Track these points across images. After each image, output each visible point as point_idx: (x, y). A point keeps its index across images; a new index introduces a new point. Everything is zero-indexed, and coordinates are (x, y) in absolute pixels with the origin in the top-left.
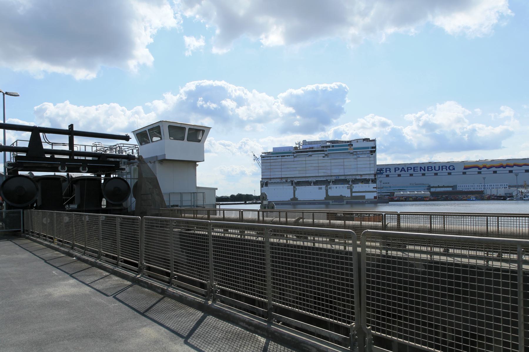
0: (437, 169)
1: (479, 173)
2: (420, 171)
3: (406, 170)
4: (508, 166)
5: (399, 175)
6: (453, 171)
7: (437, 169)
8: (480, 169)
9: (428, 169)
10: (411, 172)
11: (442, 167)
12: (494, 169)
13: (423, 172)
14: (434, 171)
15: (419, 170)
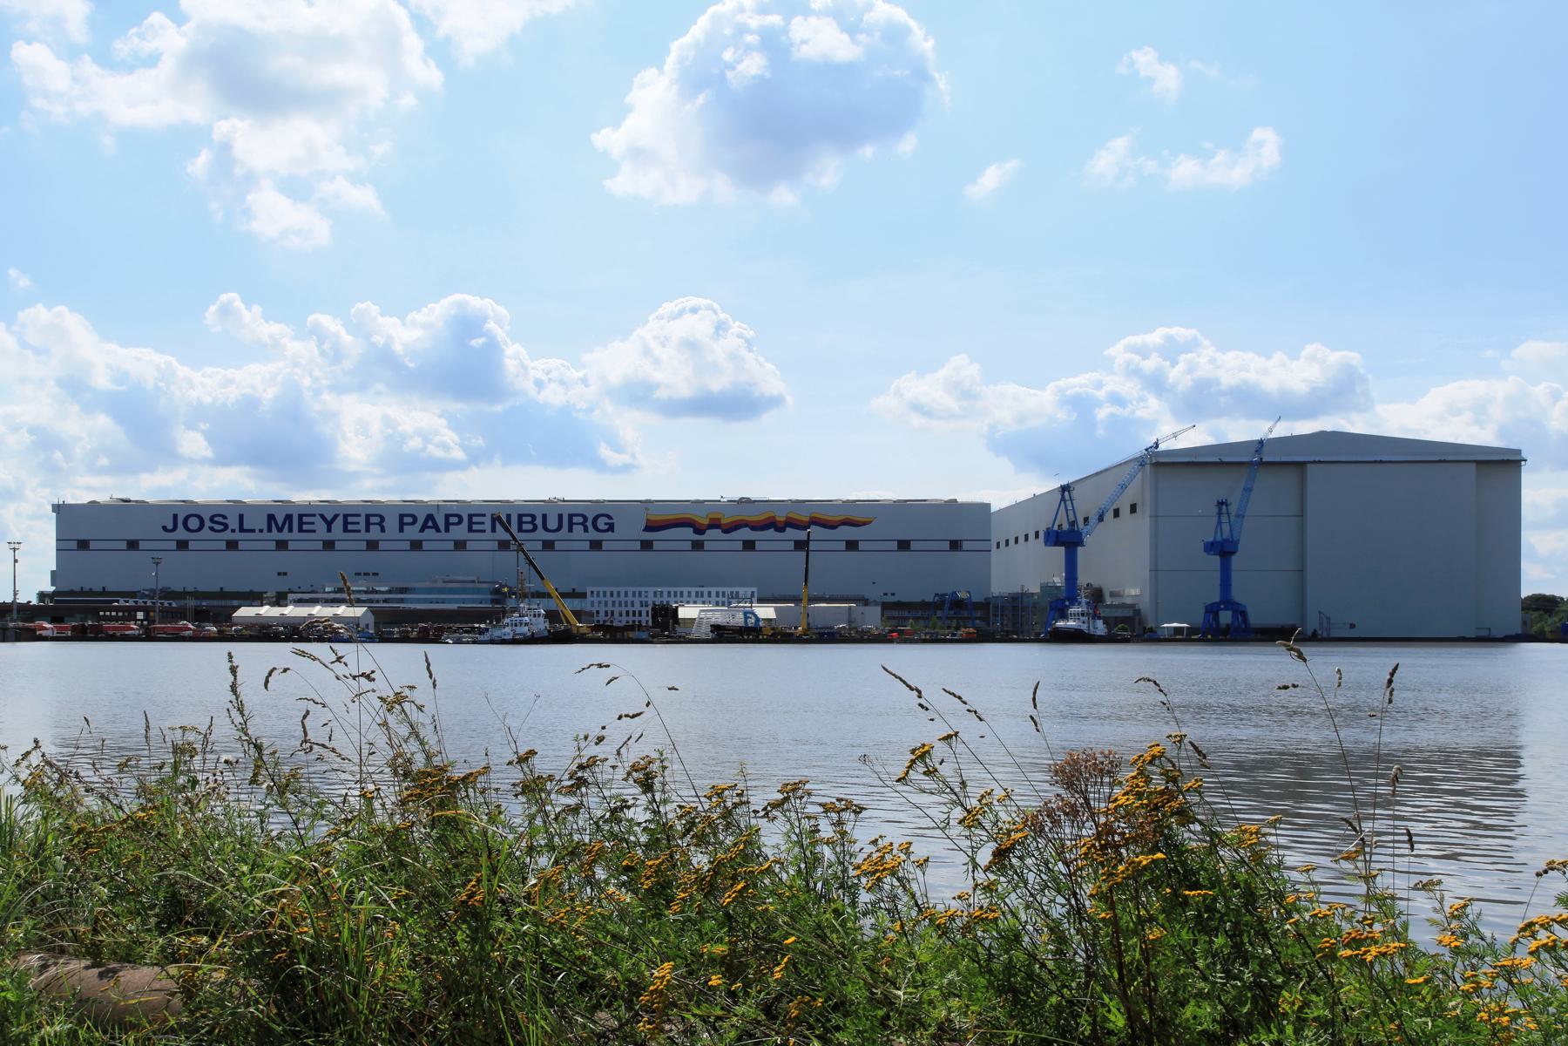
0: (552, 524)
1: (698, 546)
2: (494, 530)
3: (442, 525)
4: (791, 523)
5: (416, 545)
6: (608, 535)
7: (552, 524)
8: (699, 530)
9: (520, 523)
10: (459, 532)
11: (571, 516)
12: (745, 533)
13: (501, 534)
14: (541, 534)
15: (488, 526)
